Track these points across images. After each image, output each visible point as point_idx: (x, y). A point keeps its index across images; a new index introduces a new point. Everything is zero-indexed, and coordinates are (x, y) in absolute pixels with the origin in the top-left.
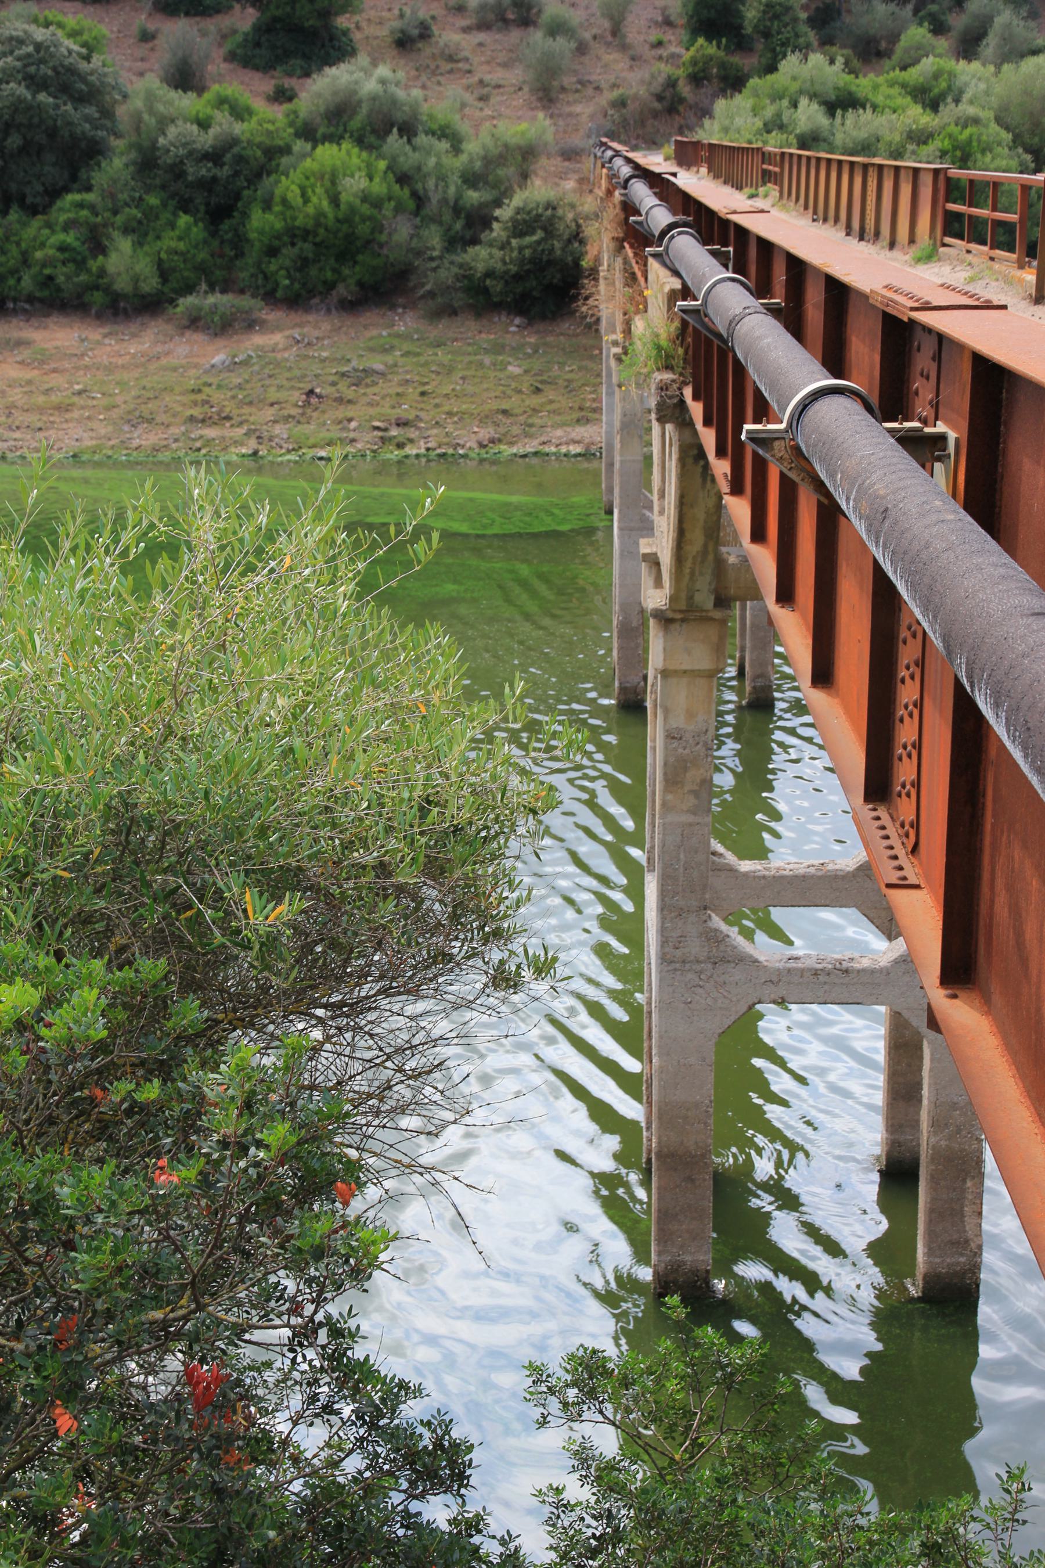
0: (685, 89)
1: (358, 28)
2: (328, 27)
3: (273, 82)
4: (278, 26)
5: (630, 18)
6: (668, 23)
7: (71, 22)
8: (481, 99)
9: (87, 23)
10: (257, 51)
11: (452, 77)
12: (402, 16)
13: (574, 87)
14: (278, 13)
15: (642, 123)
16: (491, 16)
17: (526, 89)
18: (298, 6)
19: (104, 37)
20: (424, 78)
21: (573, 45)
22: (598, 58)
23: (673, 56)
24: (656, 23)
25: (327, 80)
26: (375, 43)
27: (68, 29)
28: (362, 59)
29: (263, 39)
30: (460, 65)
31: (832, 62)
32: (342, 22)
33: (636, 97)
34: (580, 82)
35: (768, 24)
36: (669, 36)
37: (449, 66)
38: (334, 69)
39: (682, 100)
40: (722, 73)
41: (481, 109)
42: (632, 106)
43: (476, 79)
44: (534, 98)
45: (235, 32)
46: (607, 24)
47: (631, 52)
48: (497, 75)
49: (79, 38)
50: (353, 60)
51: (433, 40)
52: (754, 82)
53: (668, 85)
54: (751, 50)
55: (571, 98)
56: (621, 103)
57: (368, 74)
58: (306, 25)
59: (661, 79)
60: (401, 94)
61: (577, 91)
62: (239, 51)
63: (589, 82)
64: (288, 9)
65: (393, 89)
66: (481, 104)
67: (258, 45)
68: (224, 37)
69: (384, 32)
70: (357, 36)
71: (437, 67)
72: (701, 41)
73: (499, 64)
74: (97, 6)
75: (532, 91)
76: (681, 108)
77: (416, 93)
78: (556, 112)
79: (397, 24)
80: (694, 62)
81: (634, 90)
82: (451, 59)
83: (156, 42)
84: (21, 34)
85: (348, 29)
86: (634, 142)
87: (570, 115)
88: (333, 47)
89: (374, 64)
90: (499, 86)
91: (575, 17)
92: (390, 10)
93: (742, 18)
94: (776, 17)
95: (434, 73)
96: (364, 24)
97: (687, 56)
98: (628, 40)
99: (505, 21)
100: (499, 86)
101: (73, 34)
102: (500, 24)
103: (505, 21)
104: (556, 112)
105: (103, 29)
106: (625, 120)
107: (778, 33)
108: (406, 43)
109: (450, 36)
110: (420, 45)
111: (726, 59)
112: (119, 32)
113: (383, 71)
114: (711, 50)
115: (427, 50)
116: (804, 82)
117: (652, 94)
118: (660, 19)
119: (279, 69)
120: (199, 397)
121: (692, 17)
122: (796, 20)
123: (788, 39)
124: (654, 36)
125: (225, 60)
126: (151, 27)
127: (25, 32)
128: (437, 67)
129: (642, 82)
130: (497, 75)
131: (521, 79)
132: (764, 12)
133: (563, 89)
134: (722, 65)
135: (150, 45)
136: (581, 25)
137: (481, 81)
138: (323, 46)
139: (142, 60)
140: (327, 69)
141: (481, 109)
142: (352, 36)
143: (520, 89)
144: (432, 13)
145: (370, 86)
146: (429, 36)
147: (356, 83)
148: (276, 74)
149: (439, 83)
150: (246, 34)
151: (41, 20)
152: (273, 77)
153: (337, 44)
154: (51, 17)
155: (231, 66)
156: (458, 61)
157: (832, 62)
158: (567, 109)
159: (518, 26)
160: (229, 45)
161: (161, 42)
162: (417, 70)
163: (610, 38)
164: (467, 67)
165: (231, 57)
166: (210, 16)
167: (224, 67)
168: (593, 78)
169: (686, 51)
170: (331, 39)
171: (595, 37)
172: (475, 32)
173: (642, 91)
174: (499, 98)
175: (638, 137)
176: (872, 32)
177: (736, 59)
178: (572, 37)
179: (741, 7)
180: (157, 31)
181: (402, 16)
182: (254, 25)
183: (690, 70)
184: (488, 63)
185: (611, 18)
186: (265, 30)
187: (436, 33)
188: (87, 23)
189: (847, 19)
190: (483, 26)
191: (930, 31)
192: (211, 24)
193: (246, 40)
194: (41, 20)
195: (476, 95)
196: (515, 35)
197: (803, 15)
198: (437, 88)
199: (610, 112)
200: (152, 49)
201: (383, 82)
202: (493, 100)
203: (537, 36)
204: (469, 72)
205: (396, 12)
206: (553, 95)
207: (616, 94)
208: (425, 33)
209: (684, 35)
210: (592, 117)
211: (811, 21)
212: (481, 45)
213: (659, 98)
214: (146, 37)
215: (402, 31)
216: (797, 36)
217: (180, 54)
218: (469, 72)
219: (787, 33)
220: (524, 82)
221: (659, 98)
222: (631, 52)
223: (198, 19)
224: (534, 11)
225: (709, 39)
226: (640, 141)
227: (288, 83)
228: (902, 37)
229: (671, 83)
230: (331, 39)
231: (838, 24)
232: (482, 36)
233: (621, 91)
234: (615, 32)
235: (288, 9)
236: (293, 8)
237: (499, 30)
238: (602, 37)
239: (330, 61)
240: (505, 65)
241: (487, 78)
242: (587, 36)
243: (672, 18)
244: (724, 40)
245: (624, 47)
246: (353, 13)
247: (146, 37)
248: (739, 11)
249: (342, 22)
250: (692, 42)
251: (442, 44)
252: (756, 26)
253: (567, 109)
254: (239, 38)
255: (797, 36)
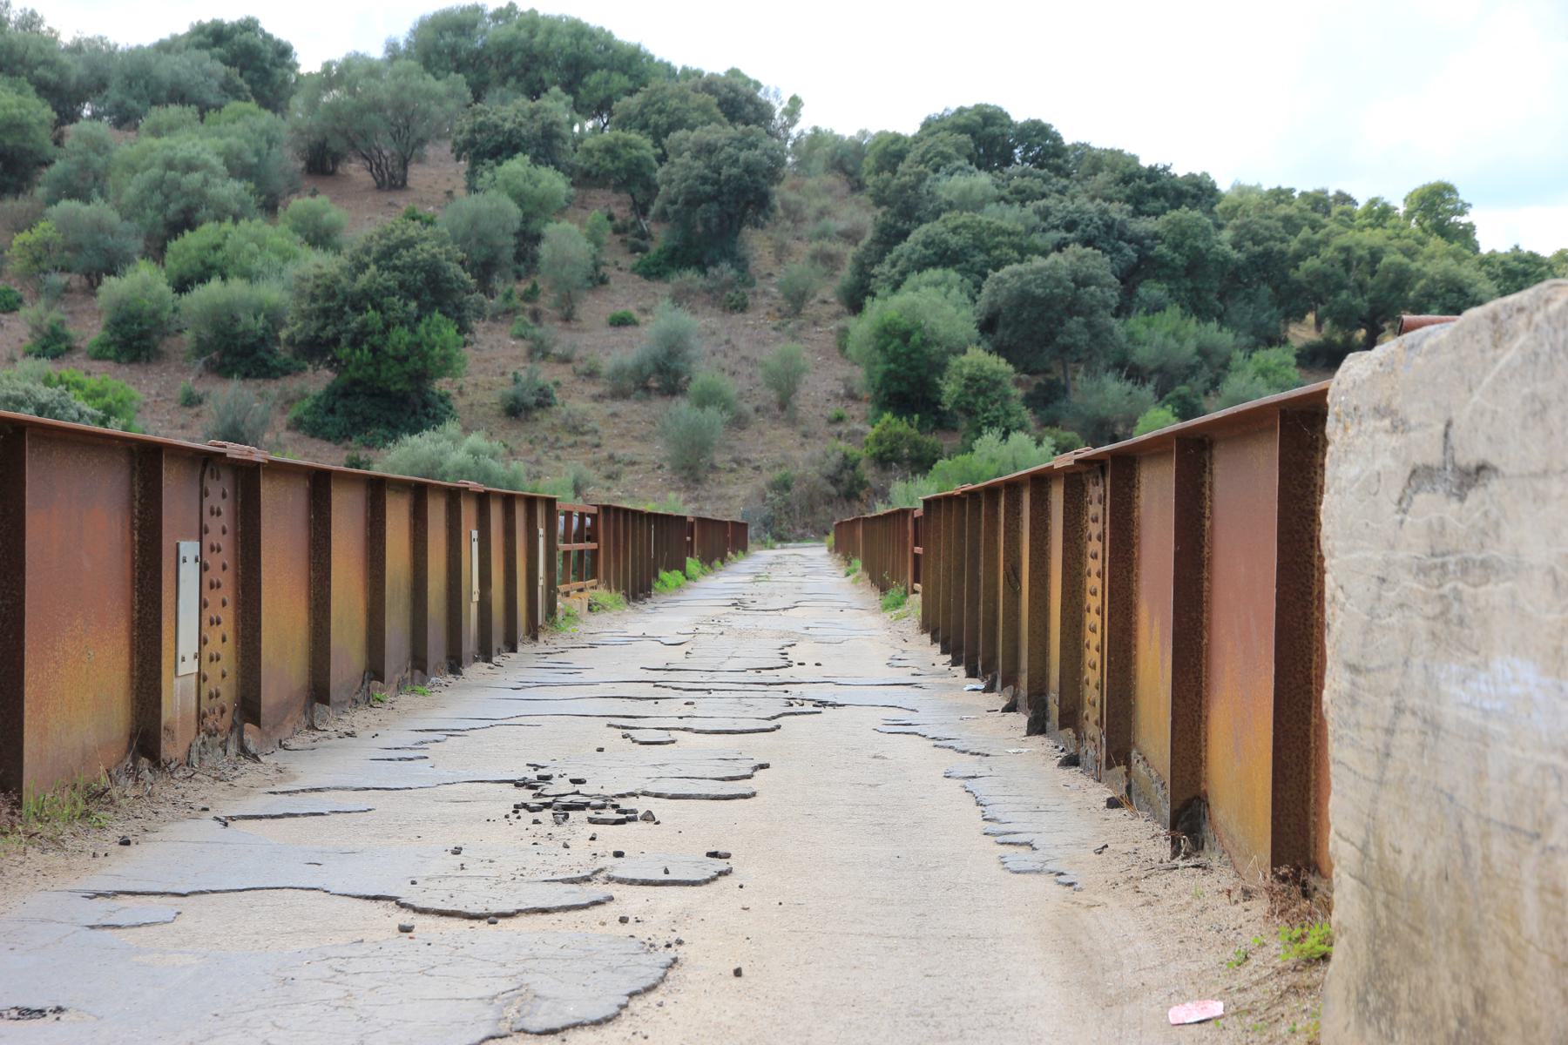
0: (869, 473)
1: (461, 392)
2: (421, 392)
3: (346, 454)
4: (358, 389)
5: (802, 390)
6: (852, 396)
7: (92, 383)
8: (609, 477)
9: (112, 383)
10: (330, 418)
11: (574, 451)
12: (516, 380)
13: (728, 466)
14: (358, 375)
15: (812, 509)
16: (630, 384)
17: (667, 466)
18: (383, 367)
19: (132, 399)
20: (539, 451)
21: (726, 416)
22: (761, 433)
23: (854, 434)
24: (837, 396)
25: (404, 450)
26: (481, 411)
27: (87, 390)
28: (452, 427)
29: (338, 404)
30: (587, 438)
31: (1039, 443)
32: (441, 385)
33: (802, 479)
34: (735, 460)
35: (972, 399)
36: (855, 409)
37: (572, 439)
38: (415, 437)
39: (862, 484)
40: (915, 454)
41: (609, 489)
42: (797, 489)
43: (605, 454)
44: (676, 478)
45: (304, 396)
46: (773, 395)
47: (803, 428)
48: (632, 450)
49: (99, 401)
50: (440, 428)
51: (555, 408)
52: (941, 464)
53: (845, 466)
54: (955, 429)
55: (724, 477)
56: (784, 485)
57: (456, 442)
58: (393, 388)
59: (835, 459)
60: (497, 467)
61: (732, 470)
62: (306, 418)
63: (749, 461)
64: (371, 370)
65: (486, 461)
66: (608, 483)
67: (332, 411)
68: (290, 402)
69: (492, 398)
70: (459, 403)
71: (557, 439)
72: (887, 416)
73: (635, 438)
74: (135, 366)
75: (674, 470)
76: (862, 494)
77: (517, 466)
78: (704, 493)
79: (510, 390)
80: (879, 441)
81: (801, 471)
82: (575, 430)
83: (203, 407)
84: (21, 393)
85: (448, 395)
86: (800, 531)
87: (720, 497)
88: (427, 415)
89: (467, 430)
90: (633, 463)
91: (731, 387)
92: (503, 374)
93: (940, 392)
94: (981, 392)
95: (552, 447)
96: (469, 389)
97: (871, 432)
98: (800, 415)
99: (647, 389)
100: (633, 463)
101: (93, 396)
102: (639, 392)
103: (647, 389)
104: (704, 493)
105: (138, 394)
106: (788, 504)
107: (985, 411)
108: (515, 411)
109: (577, 402)
110: (537, 415)
111: (920, 437)
112: (158, 395)
113: (476, 440)
114: (901, 427)
115: (546, 420)
116: (1003, 463)
117: (822, 475)
118: (842, 392)
119: (355, 438)
120: (582, 841)
121: (880, 389)
122: (1007, 397)
123: (997, 417)
124: (833, 409)
125: (288, 428)
126: (199, 389)
127: (27, 392)
128: (557, 439)
129: (812, 462)
130: (632, 450)
131: (662, 455)
132: (966, 386)
133: (714, 468)
134: (916, 446)
135: (196, 410)
136: (741, 395)
137: (611, 457)
138: (414, 413)
139: (183, 427)
140: (406, 437)
141: (609, 489)
142: (452, 402)
143: (660, 467)
144: (556, 378)
145: (458, 456)
146: (550, 405)
147: (442, 453)
148: (352, 444)
149: (558, 458)
150: (319, 399)
151: (55, 378)
152: (347, 448)
153: (432, 411)
154: (67, 376)
155: (295, 435)
156: (583, 434)
157: (1039, 443)
158: (717, 491)
159: (663, 395)
160: (294, 412)
161: (209, 408)
162: (531, 442)
163: (777, 412)
164: (596, 440)
165: (297, 425)
166: (276, 378)
167: (285, 435)
168: (753, 456)
169: (872, 427)
170: (426, 405)
171: (757, 410)
172: (608, 401)
173: (812, 472)
174: (631, 477)
175: (806, 526)
176: (1103, 413)
177: (931, 439)
178: (725, 408)
179: (938, 380)
180: (208, 393)
181: (516, 380)
182: (329, 387)
183: (875, 450)
184: (622, 436)
185: (779, 388)
186: (341, 394)
187: (559, 401)
188: (112, 383)
189: (1075, 399)
190: (620, 394)
191: (1175, 415)
192: (273, 388)
193: (316, 406)
194: (55, 378)
195: (604, 470)
196: (658, 405)
197: (1018, 392)
198: (554, 463)
199: (769, 495)
200: (197, 415)
201: (475, 452)
202: (626, 479)
203: (682, 406)
204: (597, 446)
205: (510, 376)
206: (701, 475)
207: (777, 474)
208: (544, 400)
209: (868, 408)
210: (746, 501)
211: (1029, 401)
212: (614, 415)
213: (834, 480)
214: (191, 401)
215: (516, 399)
216: (1008, 414)
217: (229, 419)
218: (597, 446)
219: (995, 410)
220: (666, 458)
221: (834, 480)
222: (803, 428)
223: (260, 381)
224: (684, 379)
225: (898, 414)
226: (808, 532)
227: (363, 454)
228: (1140, 420)
229: (848, 463)
230: (426, 405)
231: (1064, 404)
232: (619, 406)
233: (784, 471)
234: (783, 406)
235: (371, 370)
236: (378, 370)
237: (638, 400)
238: (767, 409)
239: (415, 429)
240: (643, 439)
241: (619, 453)
242: (748, 408)
243: (856, 391)
244: (916, 417)
245: (793, 422)
246: (454, 376)
247: (191, 401)
248: (937, 385)
249: (441, 385)
250: (878, 417)
251: (564, 413)
252: (956, 402)
253: (717, 491)
254: (308, 403)
255: (1008, 414)
